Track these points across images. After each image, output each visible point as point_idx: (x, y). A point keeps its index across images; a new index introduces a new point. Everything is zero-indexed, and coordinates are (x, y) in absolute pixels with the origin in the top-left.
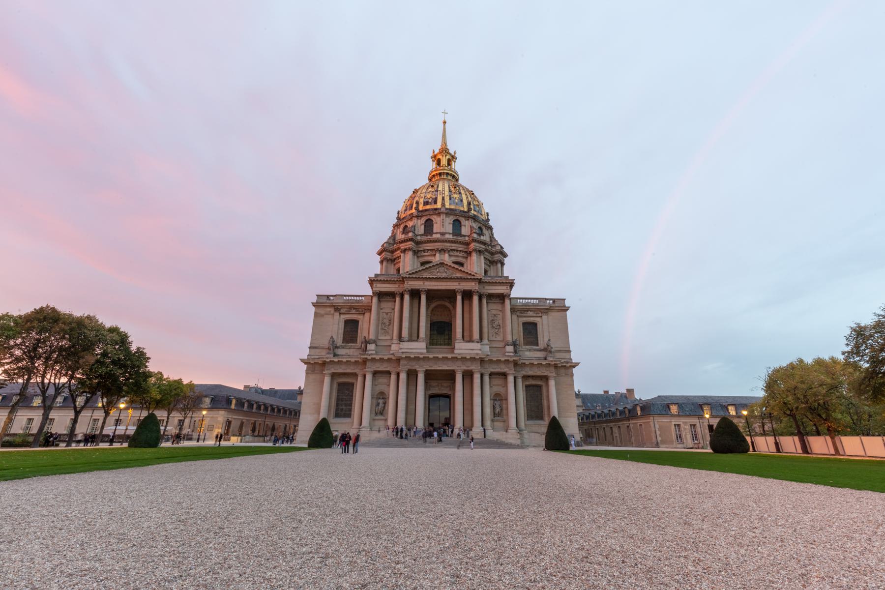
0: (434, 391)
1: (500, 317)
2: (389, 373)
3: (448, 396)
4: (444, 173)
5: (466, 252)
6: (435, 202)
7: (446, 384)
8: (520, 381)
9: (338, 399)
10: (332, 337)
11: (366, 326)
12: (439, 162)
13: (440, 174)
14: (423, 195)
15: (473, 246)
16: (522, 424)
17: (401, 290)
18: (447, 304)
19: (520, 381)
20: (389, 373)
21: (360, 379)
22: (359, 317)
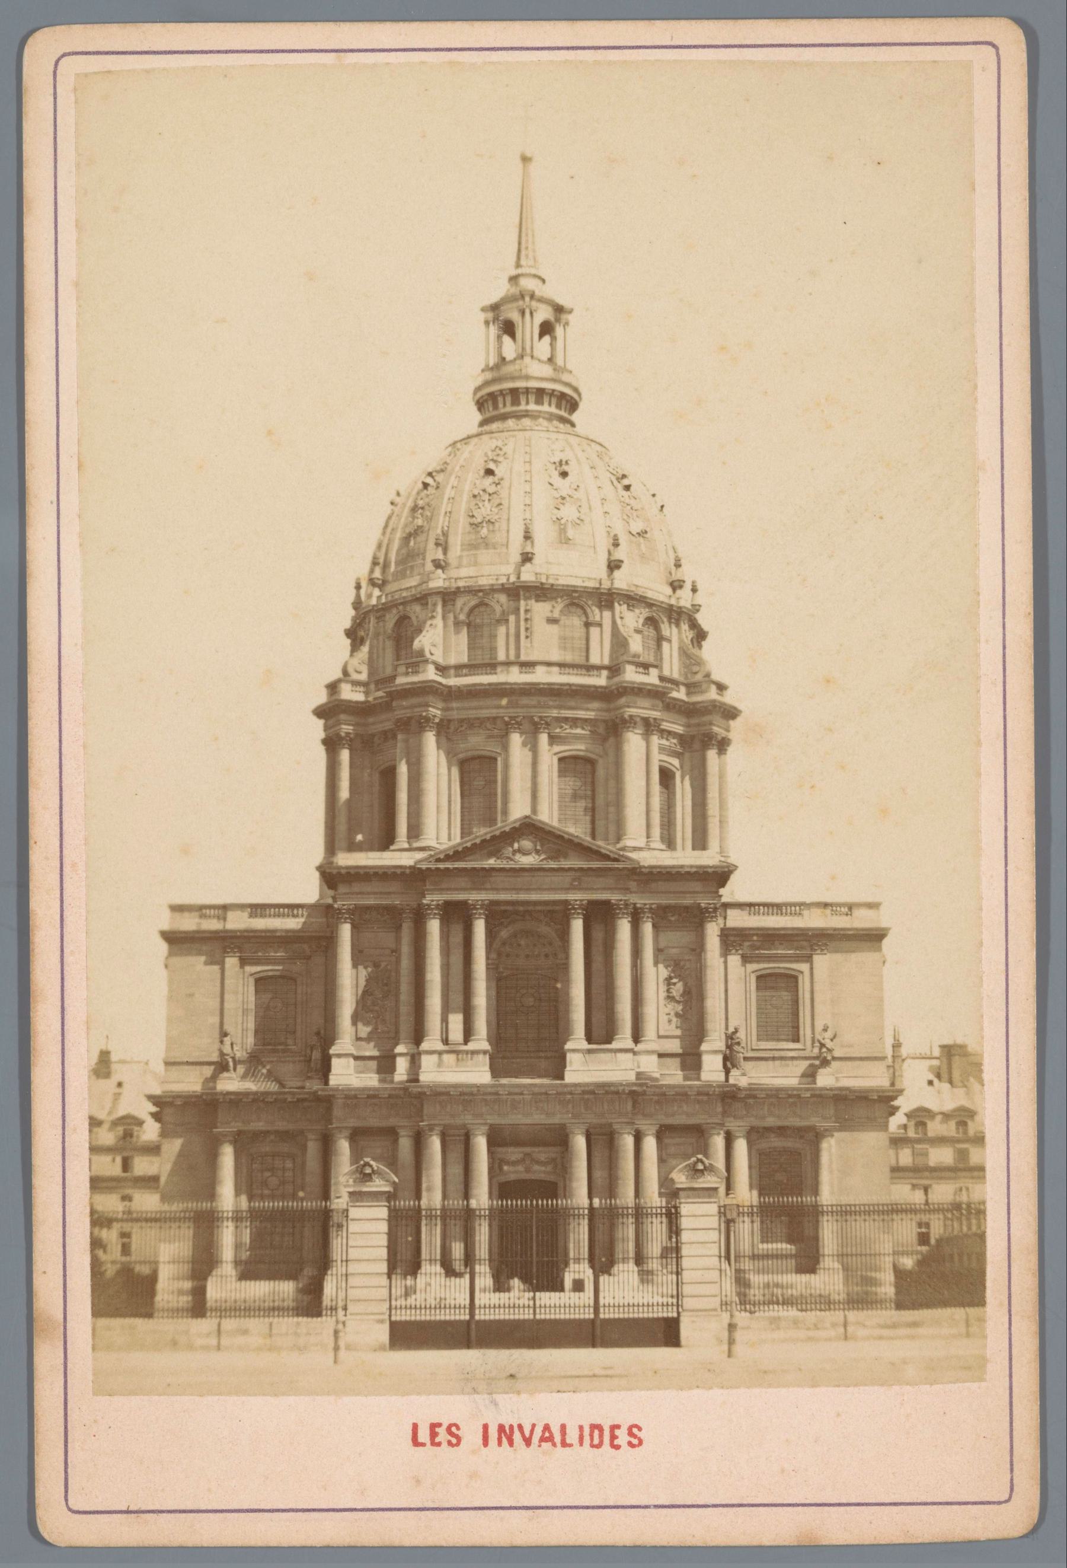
0: (512, 1173)
4: (527, 391)
7: (542, 1154)
8: (741, 1147)
12: (509, 329)
13: (515, 393)
18: (544, 929)
19: (741, 1147)
20: (392, 1133)
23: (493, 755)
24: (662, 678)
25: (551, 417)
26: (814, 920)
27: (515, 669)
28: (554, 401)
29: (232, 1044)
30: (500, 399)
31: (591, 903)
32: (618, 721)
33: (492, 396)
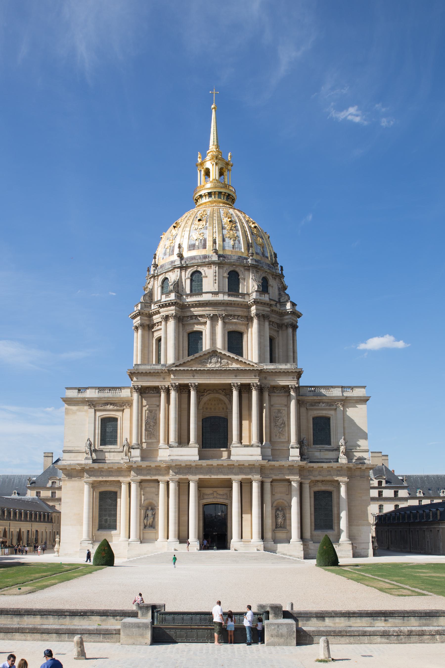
1: (285, 413)
2: (158, 482)
3: (226, 505)
5: (247, 317)
6: (204, 247)
7: (221, 491)
9: (101, 509)
10: (89, 440)
11: (126, 424)
12: (207, 173)
13: (210, 194)
14: (186, 234)
15: (253, 309)
16: (307, 535)
17: (167, 384)
18: (222, 397)
20: (158, 482)
21: (124, 487)
22: (118, 415)
23: (201, 330)
24: (270, 299)
25: (224, 203)
26: (336, 393)
27: (211, 295)
28: (225, 197)
29: (90, 445)
30: (204, 198)
31: (242, 385)
32: (252, 315)
33: (201, 196)
